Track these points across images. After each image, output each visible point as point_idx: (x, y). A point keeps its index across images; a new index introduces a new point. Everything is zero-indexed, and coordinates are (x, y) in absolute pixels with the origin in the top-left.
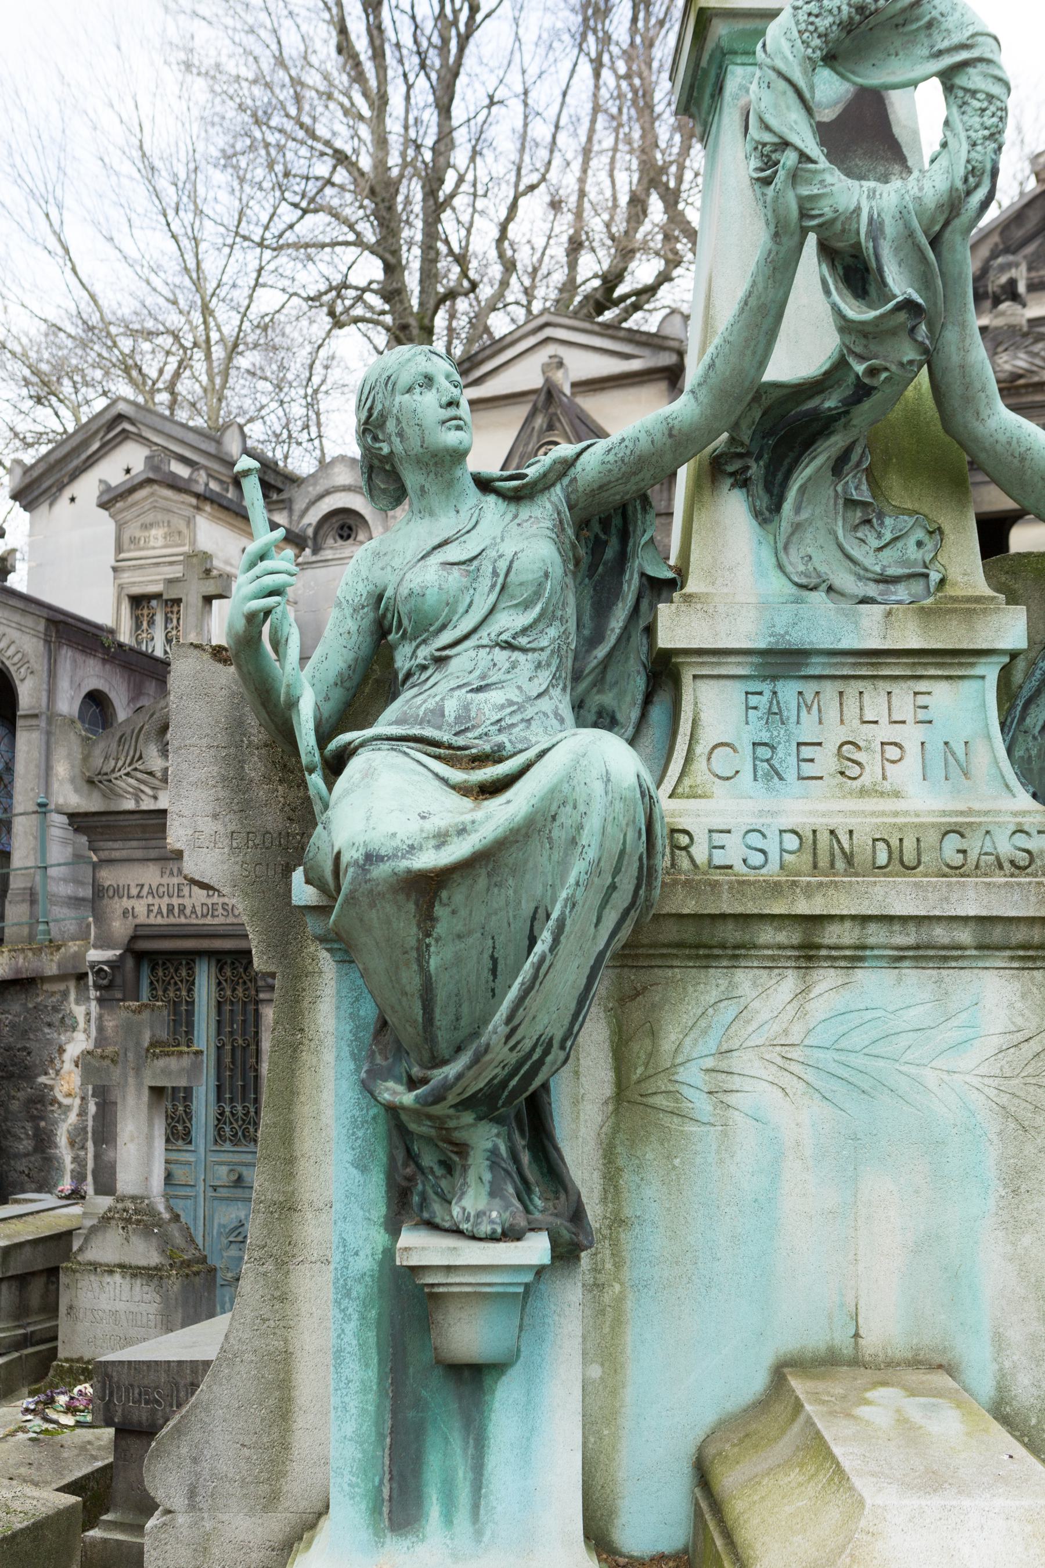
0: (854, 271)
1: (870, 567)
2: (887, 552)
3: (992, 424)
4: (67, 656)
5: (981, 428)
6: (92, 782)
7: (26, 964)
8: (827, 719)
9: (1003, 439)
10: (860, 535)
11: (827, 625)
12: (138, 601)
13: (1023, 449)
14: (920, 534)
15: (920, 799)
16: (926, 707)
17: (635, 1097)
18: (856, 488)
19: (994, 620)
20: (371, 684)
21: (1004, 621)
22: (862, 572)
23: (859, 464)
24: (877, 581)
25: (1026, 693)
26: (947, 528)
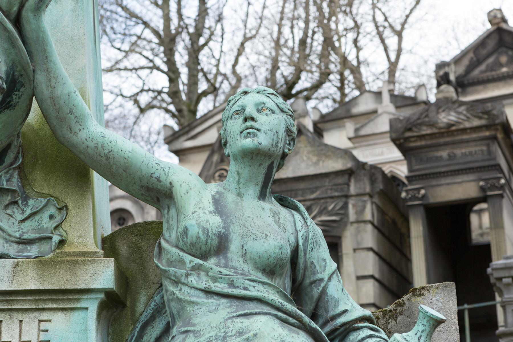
1: (12, 233)
2: (28, 223)
3: (83, 135)
5: (75, 138)
9: (91, 145)
10: (9, 212)
13: (106, 152)
14: (52, 210)
16: (47, 331)
18: (7, 181)
19: (90, 268)
21: (97, 269)
22: (8, 237)
23: (12, 164)
24: (19, 243)
25: (143, 319)
26: (71, 206)
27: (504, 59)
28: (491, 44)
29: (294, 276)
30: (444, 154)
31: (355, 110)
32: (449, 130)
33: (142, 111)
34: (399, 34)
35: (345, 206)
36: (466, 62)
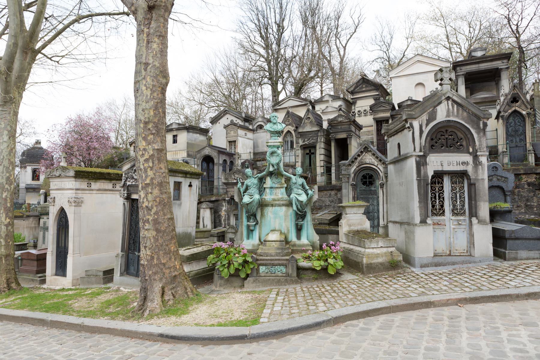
0: (273, 166)
4: (221, 155)
6: (226, 179)
7: (217, 198)
8: (274, 191)
11: (274, 185)
12: (230, 142)
15: (280, 196)
17: (262, 215)
20: (247, 189)
27: (364, 86)
28: (361, 82)
29: (303, 185)
30: (339, 127)
31: (324, 100)
32: (341, 122)
34: (345, 48)
36: (354, 87)
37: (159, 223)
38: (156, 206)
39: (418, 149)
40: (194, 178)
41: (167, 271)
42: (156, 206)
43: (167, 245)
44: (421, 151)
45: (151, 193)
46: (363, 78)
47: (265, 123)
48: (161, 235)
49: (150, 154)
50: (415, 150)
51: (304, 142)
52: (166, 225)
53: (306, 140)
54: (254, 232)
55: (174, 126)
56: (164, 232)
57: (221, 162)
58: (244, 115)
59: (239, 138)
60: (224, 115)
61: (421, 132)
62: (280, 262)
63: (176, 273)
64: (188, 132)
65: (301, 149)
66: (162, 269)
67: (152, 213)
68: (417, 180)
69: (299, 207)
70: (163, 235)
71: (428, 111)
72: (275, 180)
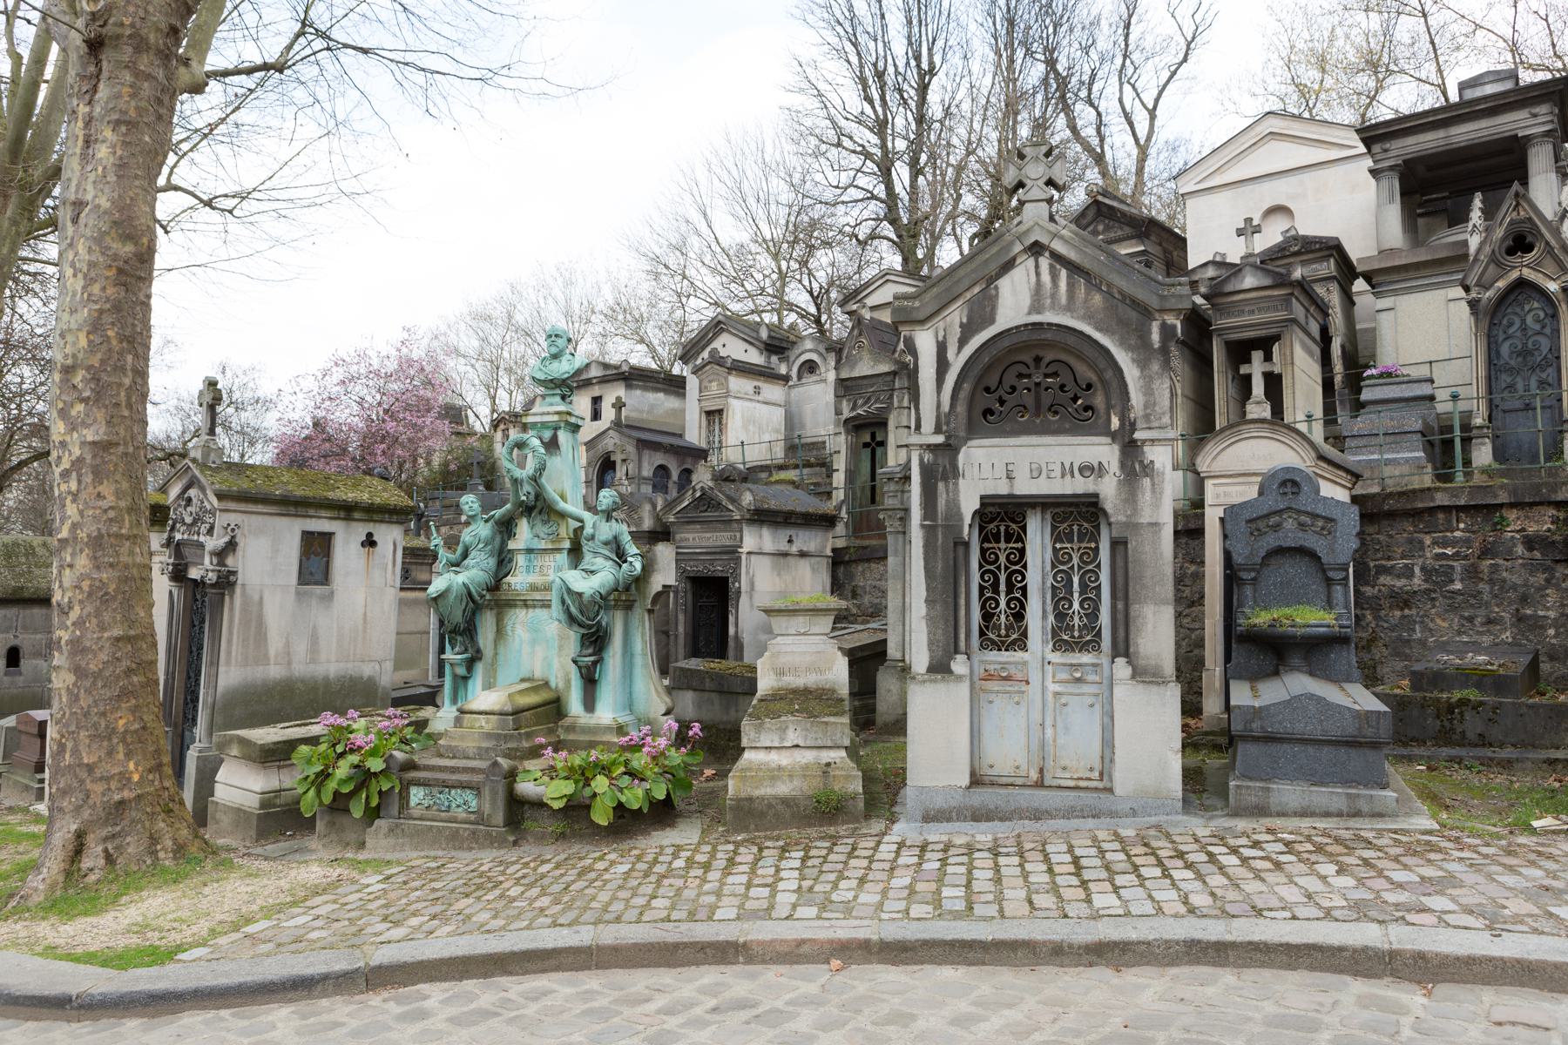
4: (646, 454)
8: (538, 561)
12: (709, 413)
17: (500, 632)
27: (1101, 228)
28: (1091, 214)
33: (863, 244)
34: (1152, 114)
35: (891, 397)
37: (84, 651)
38: (81, 602)
39: (928, 424)
40: (382, 521)
41: (99, 788)
42: (81, 602)
43: (104, 714)
44: (938, 430)
45: (71, 566)
46: (1096, 202)
47: (821, 354)
48: (87, 683)
49: (73, 458)
50: (918, 427)
51: (853, 409)
52: (104, 657)
53: (860, 402)
54: (470, 682)
55: (595, 372)
56: (97, 675)
57: (647, 472)
58: (764, 334)
59: (732, 401)
60: (716, 336)
61: (942, 365)
62: (464, 777)
63: (126, 794)
64: (629, 387)
65: (847, 432)
66: (82, 782)
67: (69, 623)
68: (922, 526)
69: (573, 610)
70: (94, 684)
71: (968, 295)
72: (542, 530)
